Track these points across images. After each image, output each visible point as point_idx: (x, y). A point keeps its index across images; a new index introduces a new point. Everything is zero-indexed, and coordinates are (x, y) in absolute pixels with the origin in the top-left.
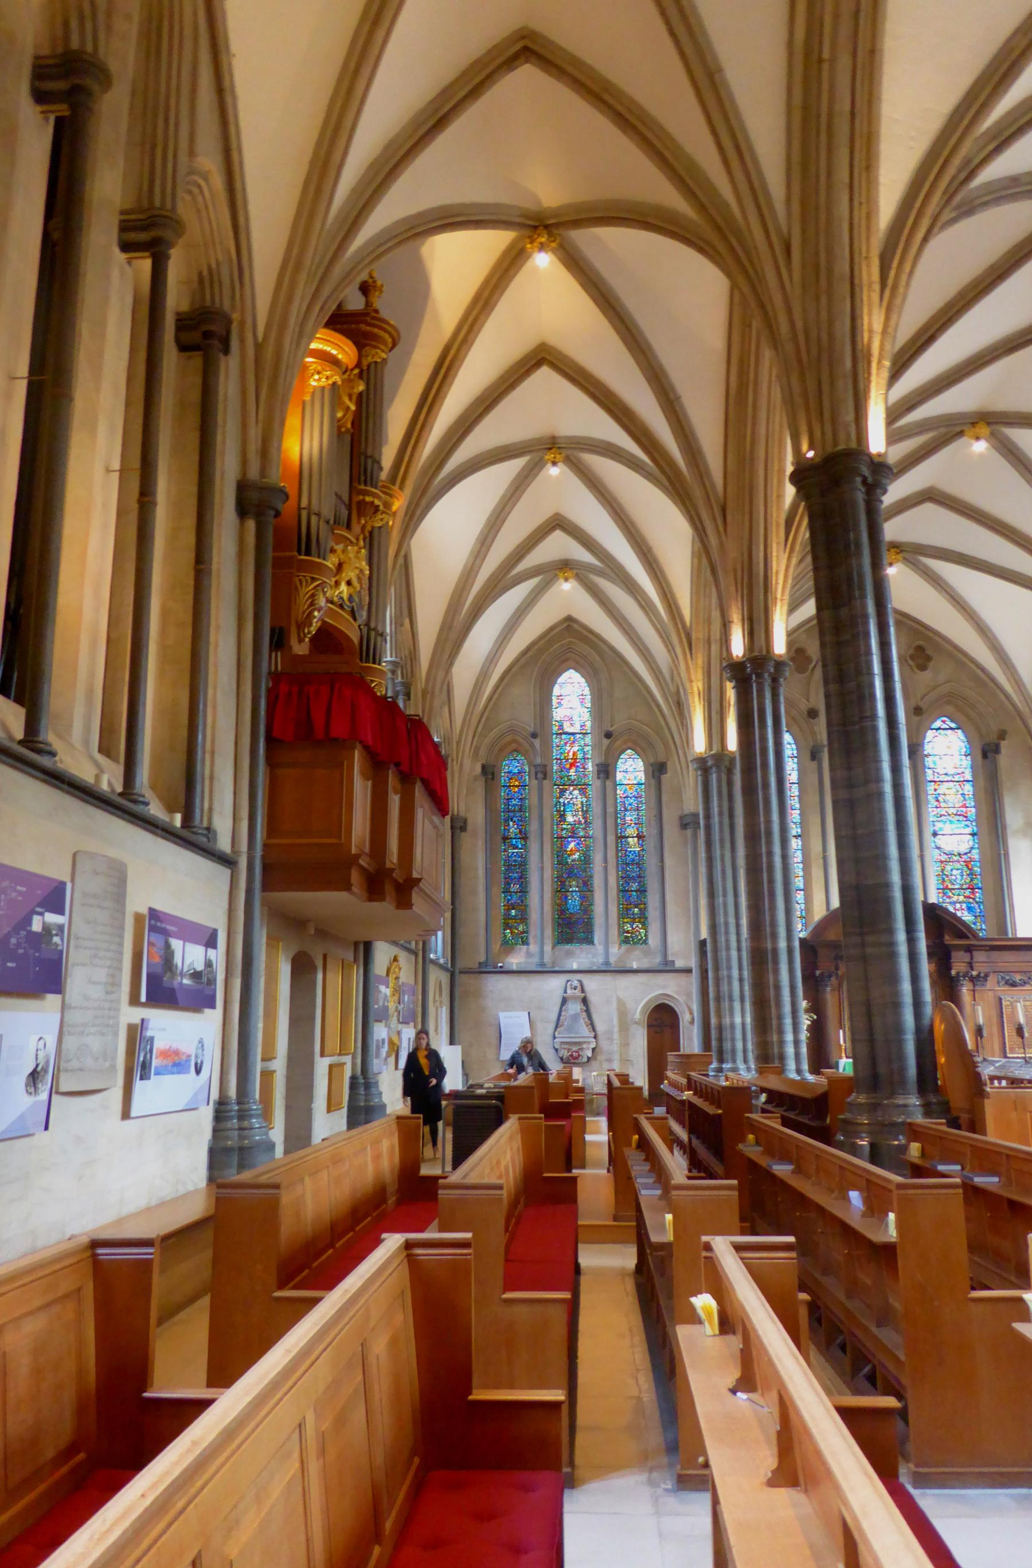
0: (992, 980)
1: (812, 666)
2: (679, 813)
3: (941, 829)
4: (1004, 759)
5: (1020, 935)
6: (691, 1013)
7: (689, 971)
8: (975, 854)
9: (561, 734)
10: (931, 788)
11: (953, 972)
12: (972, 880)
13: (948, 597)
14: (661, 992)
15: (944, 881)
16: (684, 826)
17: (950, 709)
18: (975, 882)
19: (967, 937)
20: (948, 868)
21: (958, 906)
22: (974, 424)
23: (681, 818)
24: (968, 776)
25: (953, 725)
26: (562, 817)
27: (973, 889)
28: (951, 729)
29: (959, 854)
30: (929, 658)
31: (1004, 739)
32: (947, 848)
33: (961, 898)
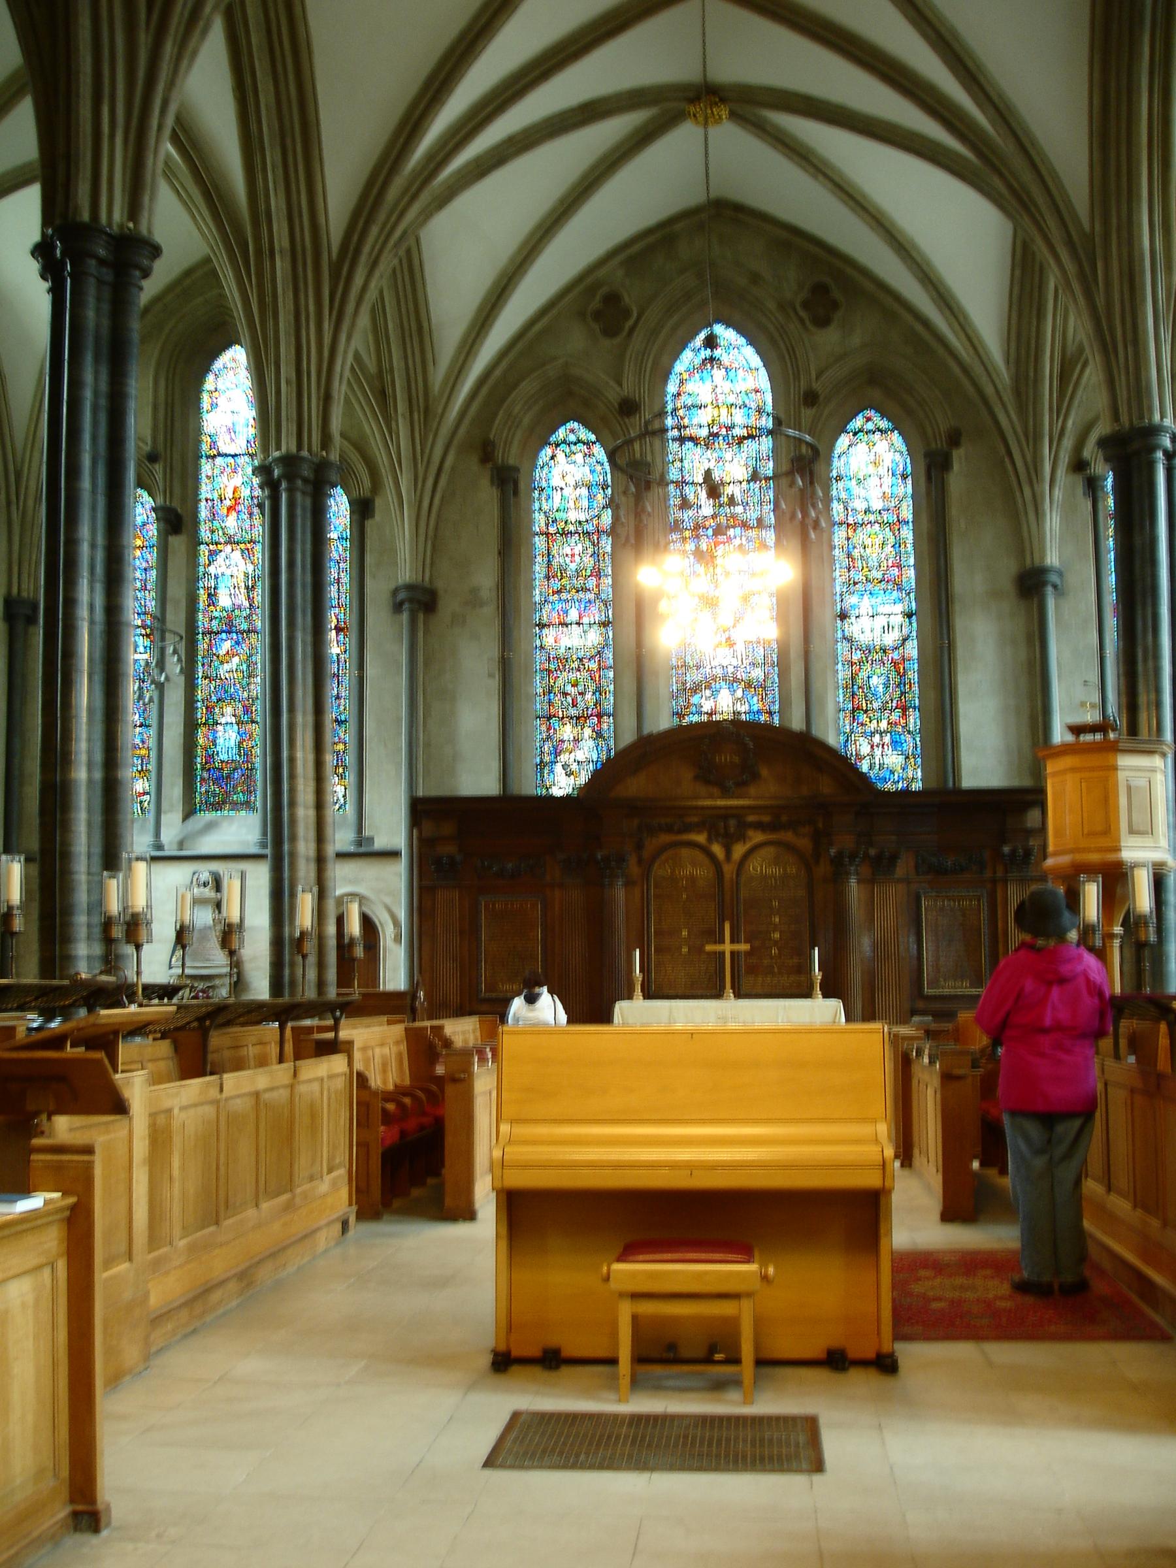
0: (903, 867)
1: (630, 322)
2: (392, 586)
4: (957, 481)
6: (396, 923)
7: (393, 854)
9: (214, 457)
10: (840, 535)
12: (903, 693)
13: (830, 185)
15: (853, 695)
16: (397, 607)
17: (876, 394)
18: (909, 696)
20: (863, 675)
21: (876, 739)
24: (907, 512)
26: (212, 596)
27: (904, 709)
30: (835, 305)
32: (864, 639)
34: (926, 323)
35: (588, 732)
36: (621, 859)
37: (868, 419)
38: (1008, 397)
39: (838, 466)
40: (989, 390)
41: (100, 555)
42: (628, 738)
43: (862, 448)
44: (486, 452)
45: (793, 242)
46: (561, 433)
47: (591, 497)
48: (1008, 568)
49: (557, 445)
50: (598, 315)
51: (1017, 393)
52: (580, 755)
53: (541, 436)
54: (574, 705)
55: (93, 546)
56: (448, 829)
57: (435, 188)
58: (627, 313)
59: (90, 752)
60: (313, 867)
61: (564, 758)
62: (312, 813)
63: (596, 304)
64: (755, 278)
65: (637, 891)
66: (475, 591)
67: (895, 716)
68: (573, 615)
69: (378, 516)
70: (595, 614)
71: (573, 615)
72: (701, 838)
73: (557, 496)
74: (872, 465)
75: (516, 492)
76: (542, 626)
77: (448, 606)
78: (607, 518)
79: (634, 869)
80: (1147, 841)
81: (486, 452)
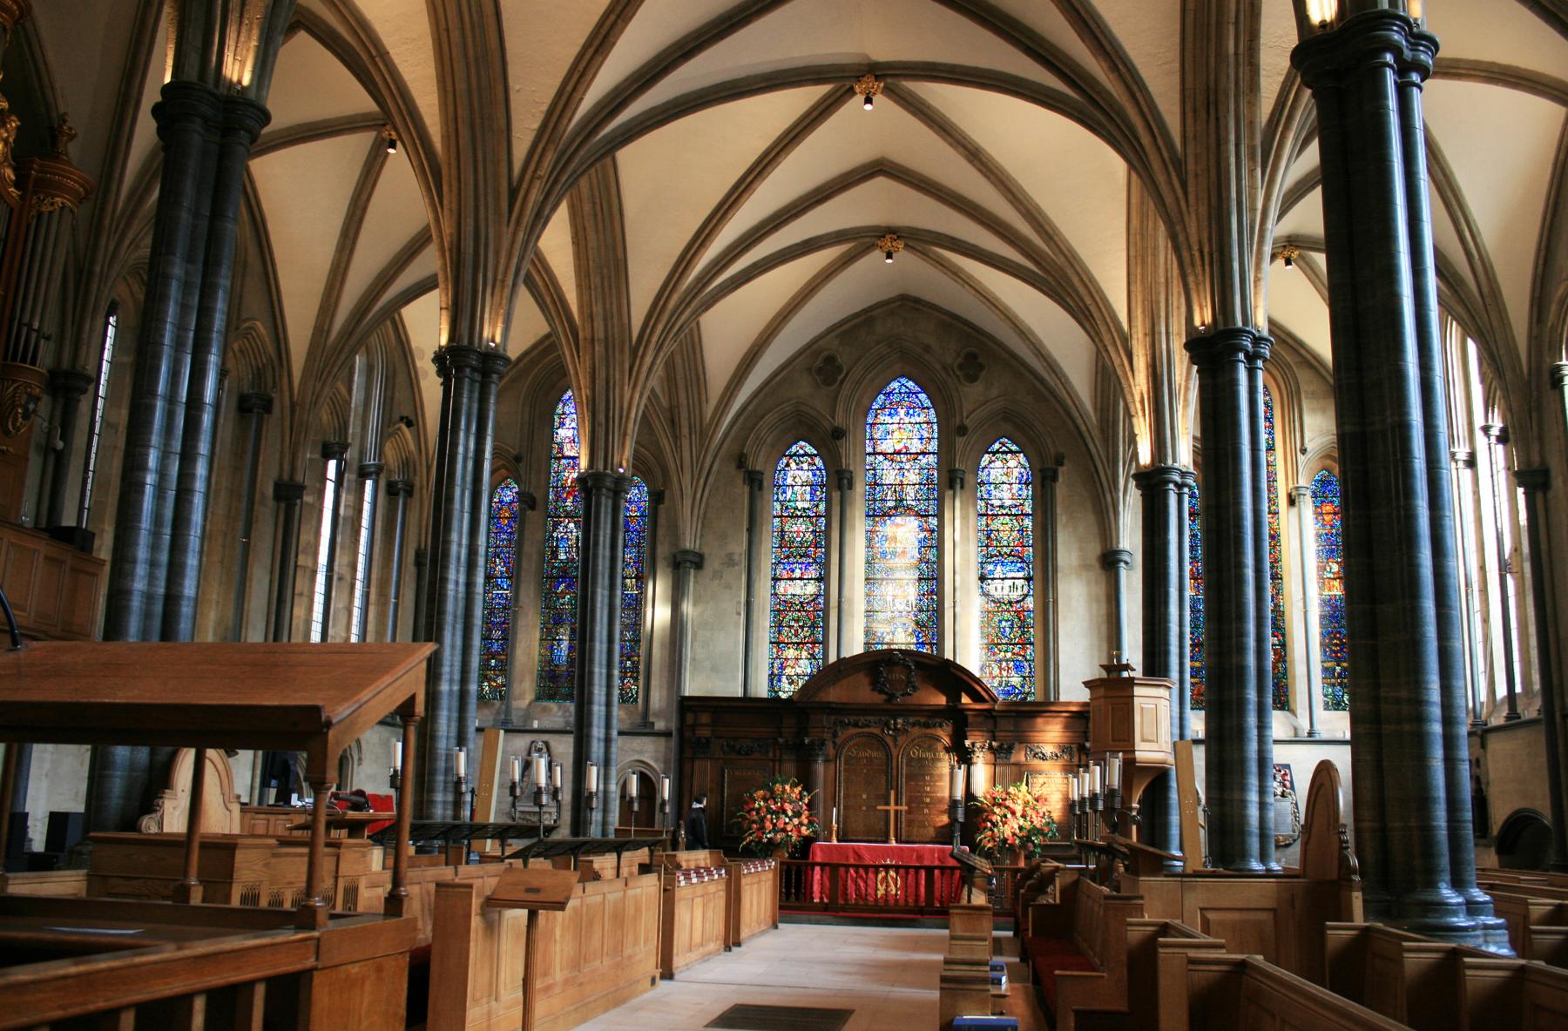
3: (992, 572)
4: (1061, 489)
5: (1062, 699)
7: (666, 734)
8: (1030, 603)
11: (967, 743)
14: (637, 757)
19: (982, 700)
22: (858, 79)
23: (675, 557)
25: (1014, 448)
26: (555, 554)
28: (1011, 452)
29: (1010, 603)
30: (981, 368)
31: (1062, 464)
32: (997, 595)
33: (1009, 655)
34: (1042, 381)
35: (804, 654)
36: (823, 744)
37: (1003, 444)
38: (1096, 433)
39: (983, 476)
40: (1083, 428)
41: (464, 551)
42: (832, 658)
43: (998, 464)
44: (741, 461)
45: (954, 325)
46: (794, 449)
47: (813, 494)
48: (1095, 549)
49: (791, 456)
50: (820, 371)
51: (1102, 430)
52: (799, 671)
53: (781, 450)
54: (796, 635)
55: (460, 545)
56: (705, 718)
57: (705, 295)
58: (840, 369)
59: (451, 672)
60: (602, 744)
61: (788, 671)
62: (603, 708)
63: (819, 363)
64: (927, 348)
65: (832, 766)
66: (730, 556)
67: (1017, 649)
68: (797, 574)
69: (667, 503)
70: (813, 572)
71: (797, 574)
72: (876, 731)
73: (789, 492)
74: (1005, 474)
75: (761, 488)
76: (776, 579)
77: (712, 564)
78: (822, 507)
79: (831, 751)
80: (1154, 746)
81: (741, 461)
